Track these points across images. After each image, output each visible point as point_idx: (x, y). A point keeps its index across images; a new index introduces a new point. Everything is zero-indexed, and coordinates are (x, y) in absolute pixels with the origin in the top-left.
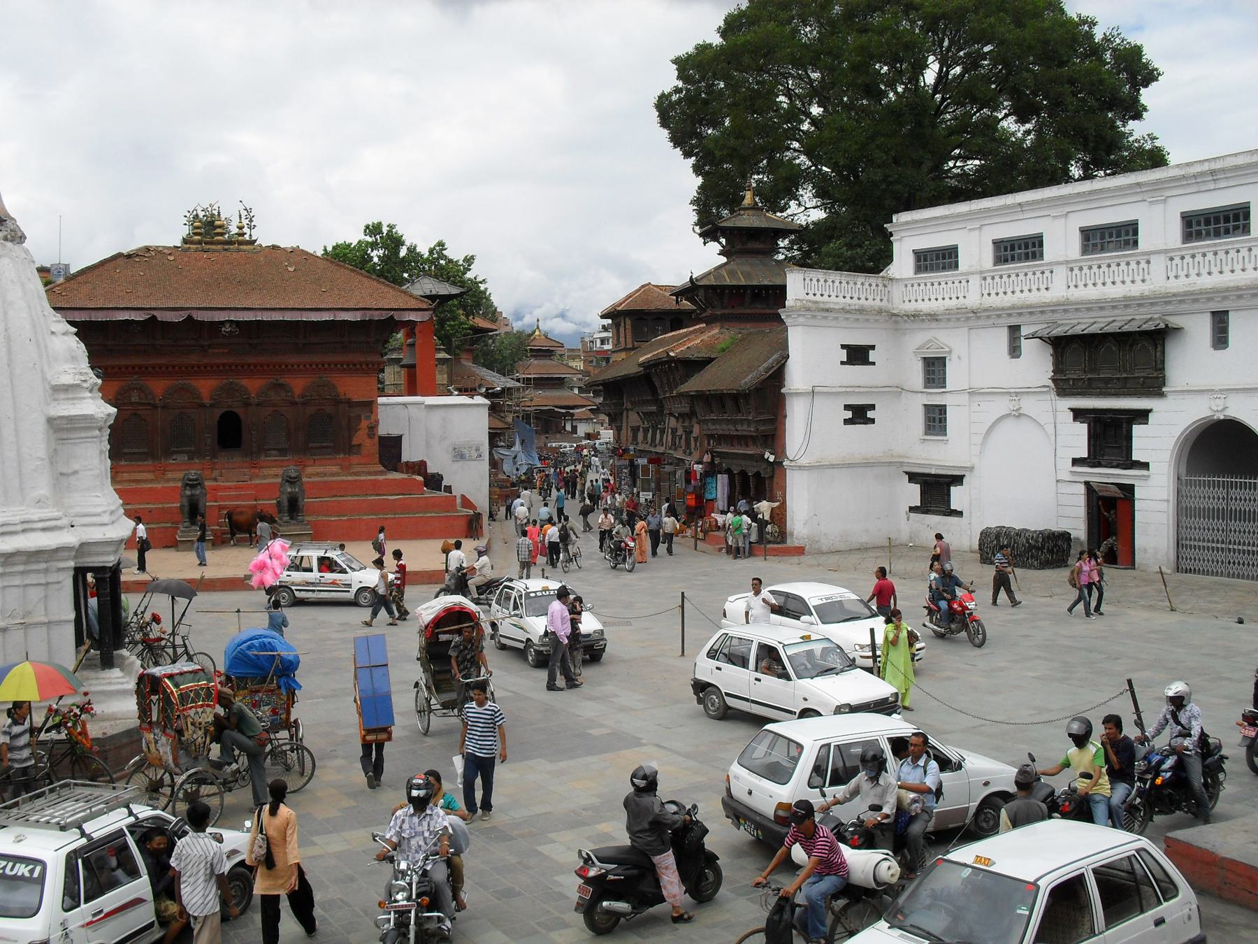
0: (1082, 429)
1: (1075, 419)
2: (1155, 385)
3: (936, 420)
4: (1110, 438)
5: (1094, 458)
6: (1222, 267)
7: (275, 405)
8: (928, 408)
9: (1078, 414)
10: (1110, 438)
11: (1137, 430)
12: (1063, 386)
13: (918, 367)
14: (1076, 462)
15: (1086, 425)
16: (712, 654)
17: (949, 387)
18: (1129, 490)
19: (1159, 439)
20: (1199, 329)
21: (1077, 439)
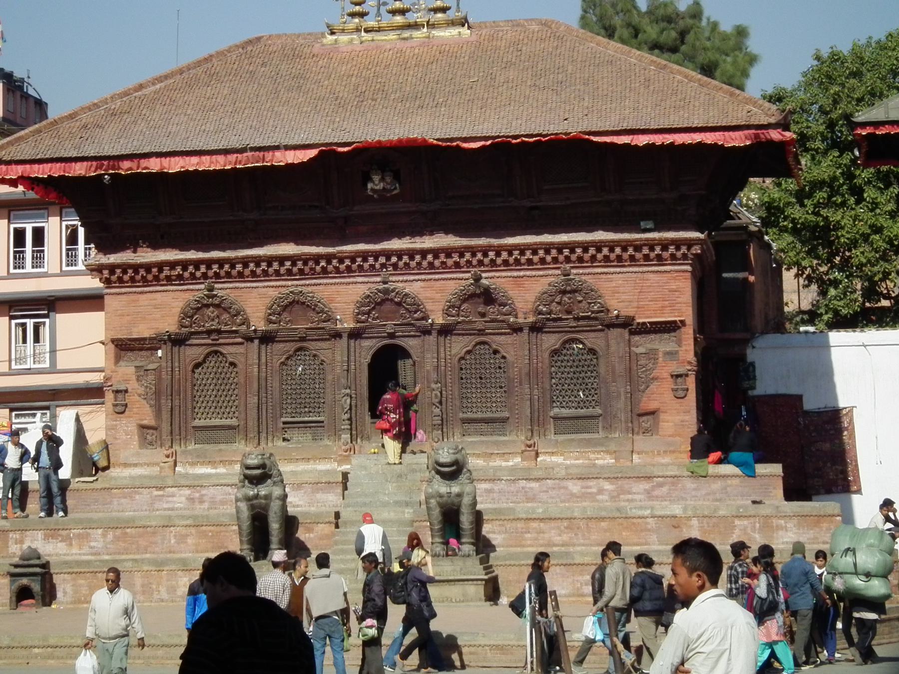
7: (481, 332)
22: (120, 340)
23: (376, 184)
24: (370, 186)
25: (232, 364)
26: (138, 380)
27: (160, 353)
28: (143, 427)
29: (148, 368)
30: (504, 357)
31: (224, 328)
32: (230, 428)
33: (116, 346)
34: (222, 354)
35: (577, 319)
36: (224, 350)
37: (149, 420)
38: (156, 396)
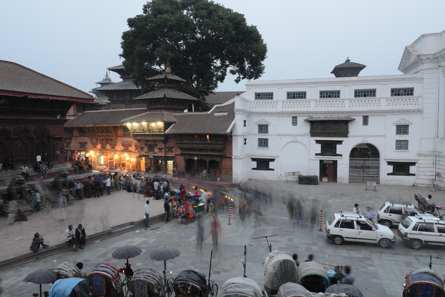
0: (319, 146)
1: (316, 143)
2: (345, 134)
3: (263, 143)
4: (329, 148)
5: (323, 153)
6: (364, 105)
8: (260, 140)
9: (317, 142)
10: (329, 148)
11: (338, 146)
12: (313, 134)
13: (257, 128)
14: (316, 154)
15: (320, 145)
16: (336, 226)
17: (269, 134)
18: (335, 162)
19: (345, 148)
20: (359, 120)
21: (318, 148)
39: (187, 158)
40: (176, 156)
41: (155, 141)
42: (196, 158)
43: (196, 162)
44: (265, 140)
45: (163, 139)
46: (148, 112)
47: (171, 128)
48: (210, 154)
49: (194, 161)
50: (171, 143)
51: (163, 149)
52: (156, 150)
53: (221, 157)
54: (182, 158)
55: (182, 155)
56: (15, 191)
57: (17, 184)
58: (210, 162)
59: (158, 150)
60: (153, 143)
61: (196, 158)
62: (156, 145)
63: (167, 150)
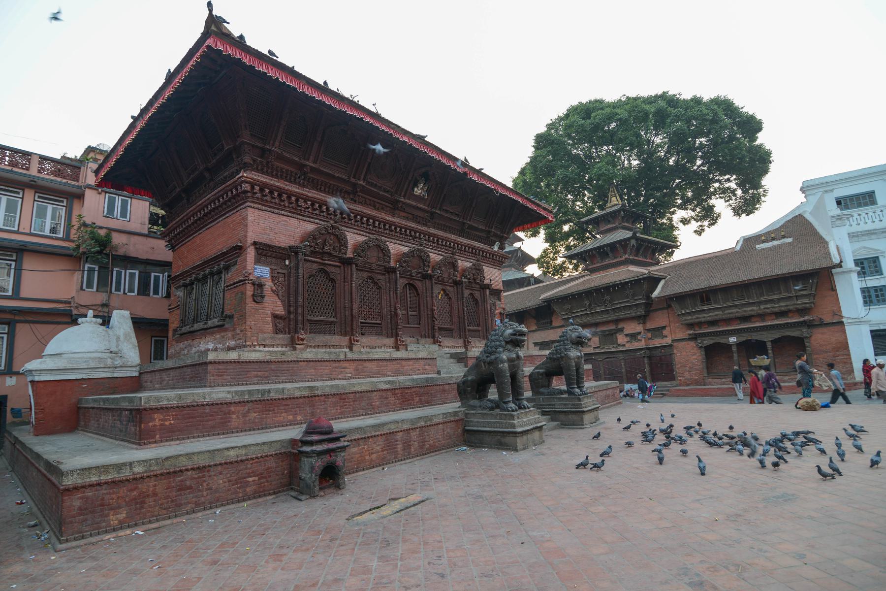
22: (260, 244)
23: (417, 191)
24: (416, 189)
25: (332, 280)
26: (273, 280)
27: (287, 262)
28: (275, 317)
29: (280, 271)
30: (450, 298)
31: (335, 253)
32: (333, 323)
33: (256, 248)
34: (327, 273)
35: (476, 283)
36: (327, 269)
37: (281, 311)
38: (289, 296)
39: (707, 342)
40: (675, 344)
41: (617, 321)
42: (733, 340)
43: (734, 349)
44: (876, 291)
45: (641, 312)
46: (588, 277)
47: (663, 287)
48: (775, 322)
49: (728, 346)
50: (659, 319)
51: (640, 333)
52: (621, 339)
53: (810, 325)
54: (692, 344)
55: (694, 338)
56: (506, 365)
57: (509, 346)
58: (774, 342)
59: (626, 339)
60: (613, 327)
61: (733, 340)
62: (622, 330)
63: (649, 335)
